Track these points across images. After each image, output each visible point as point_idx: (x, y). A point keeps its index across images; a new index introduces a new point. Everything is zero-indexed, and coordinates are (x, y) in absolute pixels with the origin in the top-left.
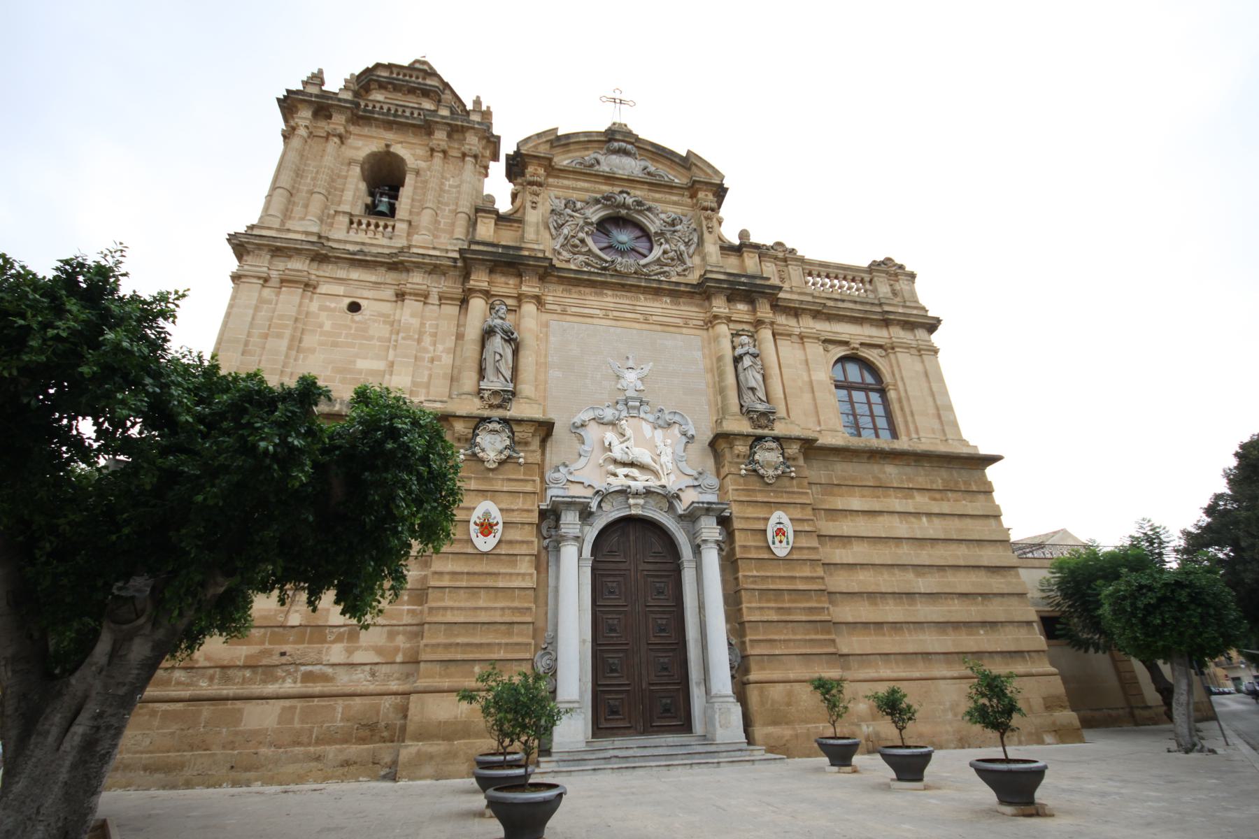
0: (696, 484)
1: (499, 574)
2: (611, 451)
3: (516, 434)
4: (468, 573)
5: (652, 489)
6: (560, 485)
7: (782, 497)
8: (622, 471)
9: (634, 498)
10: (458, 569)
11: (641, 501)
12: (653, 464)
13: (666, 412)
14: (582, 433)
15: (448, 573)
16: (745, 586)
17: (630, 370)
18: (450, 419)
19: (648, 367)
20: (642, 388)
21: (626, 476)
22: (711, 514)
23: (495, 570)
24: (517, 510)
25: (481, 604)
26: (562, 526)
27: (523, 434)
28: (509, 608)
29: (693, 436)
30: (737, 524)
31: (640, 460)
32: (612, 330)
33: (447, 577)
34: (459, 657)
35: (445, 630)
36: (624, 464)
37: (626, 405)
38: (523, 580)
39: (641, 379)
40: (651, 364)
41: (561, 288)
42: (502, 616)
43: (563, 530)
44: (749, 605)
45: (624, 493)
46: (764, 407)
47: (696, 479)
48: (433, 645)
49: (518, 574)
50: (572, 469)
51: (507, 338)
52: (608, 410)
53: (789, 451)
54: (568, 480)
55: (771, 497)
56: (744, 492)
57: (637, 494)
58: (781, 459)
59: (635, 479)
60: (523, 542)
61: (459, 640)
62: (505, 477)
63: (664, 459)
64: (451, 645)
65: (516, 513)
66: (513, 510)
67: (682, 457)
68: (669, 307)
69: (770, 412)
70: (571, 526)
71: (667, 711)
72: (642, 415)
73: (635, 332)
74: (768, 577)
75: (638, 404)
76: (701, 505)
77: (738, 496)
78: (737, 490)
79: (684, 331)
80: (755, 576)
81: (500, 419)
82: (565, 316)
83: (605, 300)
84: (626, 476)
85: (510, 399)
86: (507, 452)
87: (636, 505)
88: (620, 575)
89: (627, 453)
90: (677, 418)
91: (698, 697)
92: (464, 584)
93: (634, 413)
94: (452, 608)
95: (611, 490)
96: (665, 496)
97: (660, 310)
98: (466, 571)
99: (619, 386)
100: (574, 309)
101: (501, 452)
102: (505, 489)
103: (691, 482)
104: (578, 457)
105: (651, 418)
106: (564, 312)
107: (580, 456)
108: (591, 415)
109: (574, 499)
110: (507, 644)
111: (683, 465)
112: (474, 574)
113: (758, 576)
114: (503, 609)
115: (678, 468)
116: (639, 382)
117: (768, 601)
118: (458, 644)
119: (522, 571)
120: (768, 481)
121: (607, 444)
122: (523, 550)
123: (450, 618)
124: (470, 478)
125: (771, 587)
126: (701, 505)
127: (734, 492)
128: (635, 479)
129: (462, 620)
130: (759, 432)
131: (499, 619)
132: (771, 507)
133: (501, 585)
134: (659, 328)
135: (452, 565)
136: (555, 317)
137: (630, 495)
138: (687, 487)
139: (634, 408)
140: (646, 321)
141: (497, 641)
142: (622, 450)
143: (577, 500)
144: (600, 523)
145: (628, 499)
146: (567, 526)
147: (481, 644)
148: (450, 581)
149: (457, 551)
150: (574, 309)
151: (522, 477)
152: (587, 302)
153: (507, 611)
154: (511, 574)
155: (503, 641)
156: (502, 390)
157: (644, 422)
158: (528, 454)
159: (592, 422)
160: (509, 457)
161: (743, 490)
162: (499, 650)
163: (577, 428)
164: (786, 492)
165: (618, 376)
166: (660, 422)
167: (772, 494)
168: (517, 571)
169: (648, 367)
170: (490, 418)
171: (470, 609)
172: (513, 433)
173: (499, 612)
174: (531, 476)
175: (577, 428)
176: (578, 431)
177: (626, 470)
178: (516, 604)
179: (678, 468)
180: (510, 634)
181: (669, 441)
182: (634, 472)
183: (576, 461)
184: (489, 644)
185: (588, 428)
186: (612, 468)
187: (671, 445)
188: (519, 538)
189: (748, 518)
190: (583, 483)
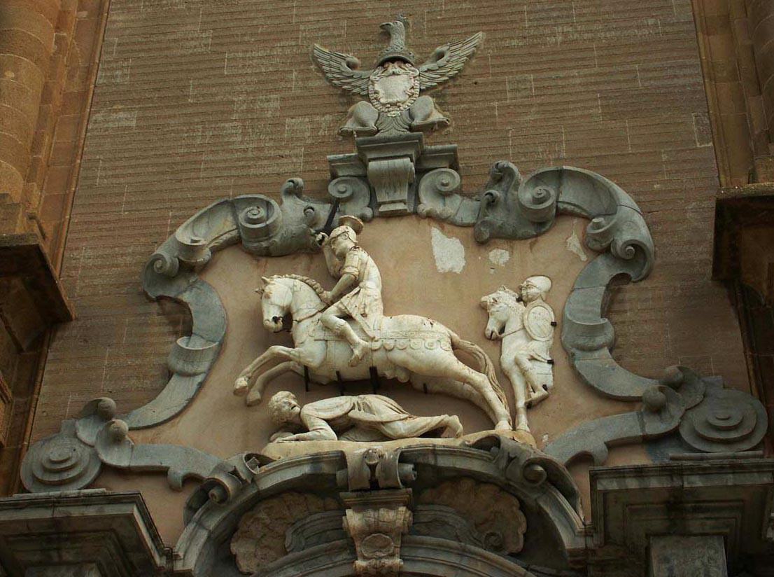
0: (656, 427)
2: (291, 343)
5: (443, 462)
9: (361, 507)
11: (398, 516)
14: (186, 297)
17: (393, 68)
20: (437, 116)
21: (343, 426)
22: (695, 524)
29: (638, 247)
31: (398, 356)
36: (342, 385)
37: (364, 178)
39: (435, 91)
47: (657, 410)
50: (123, 424)
52: (289, 202)
54: (106, 469)
57: (374, 485)
63: (514, 348)
67: (593, 331)
72: (428, 204)
75: (406, 163)
76: (632, 484)
87: (373, 532)
89: (342, 337)
90: (570, 195)
93: (397, 199)
95: (268, 483)
96: (505, 488)
99: (350, 125)
103: (626, 424)
107: (169, 374)
108: (224, 226)
111: (598, 364)
116: (429, 100)
121: (271, 313)
126: (632, 484)
128: (376, 431)
137: (347, 496)
139: (394, 179)
142: (327, 327)
145: (342, 508)
157: (436, 232)
159: (227, 257)
163: (168, 278)
165: (345, 93)
166: (497, 217)
169: (455, 56)
175: (168, 278)
176: (171, 293)
177: (338, 405)
179: (578, 376)
181: (540, 284)
183: (154, 393)
185: (211, 278)
186: (282, 399)
187: (547, 298)
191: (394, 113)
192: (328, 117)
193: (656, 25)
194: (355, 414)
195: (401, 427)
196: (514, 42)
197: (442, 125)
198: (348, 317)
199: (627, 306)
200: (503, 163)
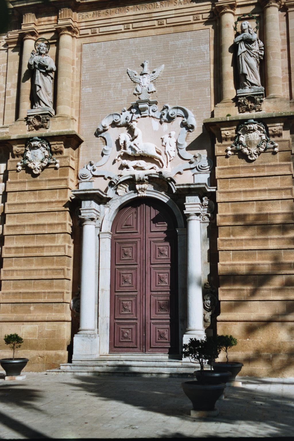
0: (192, 166)
1: (44, 247)
3: (52, 146)
4: (25, 247)
5: (153, 176)
6: (87, 180)
7: (263, 171)
8: (131, 163)
10: (20, 245)
12: (158, 155)
13: (170, 107)
14: (105, 137)
15: (14, 248)
16: (222, 248)
18: (9, 142)
19: (160, 70)
21: (135, 167)
23: (42, 245)
24: (55, 202)
25: (34, 267)
26: (81, 211)
27: (57, 145)
28: (50, 269)
30: (219, 198)
32: (131, 41)
33: (13, 251)
34: (21, 301)
35: (13, 284)
38: (59, 250)
40: (163, 66)
41: (91, 13)
42: (46, 274)
43: (82, 215)
44: (223, 263)
45: (132, 182)
46: (252, 90)
48: (7, 294)
49: (56, 246)
51: (44, 71)
53: (273, 128)
55: (253, 172)
56: (228, 171)
58: (264, 137)
59: (142, 169)
60: (58, 224)
61: (21, 290)
62: (47, 179)
64: (16, 293)
65: (54, 204)
66: (52, 202)
68: (183, 6)
69: (257, 95)
70: (87, 211)
71: (160, 336)
73: (150, 38)
74: (242, 240)
77: (223, 174)
78: (222, 169)
79: (195, 26)
80: (231, 240)
81: (39, 137)
82: (95, 38)
83: (127, 14)
84: (135, 167)
85: (48, 120)
86: (46, 162)
88: (133, 243)
91: (182, 329)
92: (23, 255)
94: (17, 270)
97: (174, 12)
98: (24, 246)
100: (102, 30)
101: (42, 162)
102: (47, 187)
103: (187, 165)
104: (100, 156)
105: (157, 115)
106: (94, 34)
109: (86, 192)
110: (49, 293)
112: (29, 247)
113: (234, 240)
114: (46, 270)
115: (179, 154)
116: (152, 84)
117: (241, 259)
118: (20, 293)
119: (58, 244)
120: (251, 159)
122: (59, 229)
123: (15, 277)
124: (24, 182)
125: (244, 248)
127: (220, 171)
128: (142, 169)
129: (22, 277)
130: (247, 114)
131: (44, 277)
132: (253, 181)
133: (45, 254)
134: (172, 29)
135: (16, 243)
136: (87, 40)
138: (184, 170)
140: (161, 26)
141: (43, 291)
143: (89, 192)
144: (115, 205)
146: (85, 211)
147: (34, 293)
148: (15, 253)
149: (18, 233)
150: (102, 30)
151: (58, 178)
152: (112, 20)
153: (49, 271)
154: (51, 247)
155: (46, 291)
156: (42, 114)
158: (63, 160)
160: (49, 164)
161: (228, 168)
162: (45, 297)
164: (268, 166)
167: (254, 169)
168: (55, 244)
170: (32, 138)
171: (27, 270)
172: (50, 145)
173: (44, 272)
174: (64, 175)
177: (135, 163)
178: (55, 267)
180: (51, 286)
182: (142, 163)
184: (38, 293)
188: (56, 222)
189: (230, 192)
190: (103, 176)
191: (145, 88)
192: (131, 89)
193: (201, 62)
194: (137, 165)
195: (145, 168)
196: (171, 67)
197: (155, 91)
198: (135, 145)
199: (190, 138)
200: (167, 105)
